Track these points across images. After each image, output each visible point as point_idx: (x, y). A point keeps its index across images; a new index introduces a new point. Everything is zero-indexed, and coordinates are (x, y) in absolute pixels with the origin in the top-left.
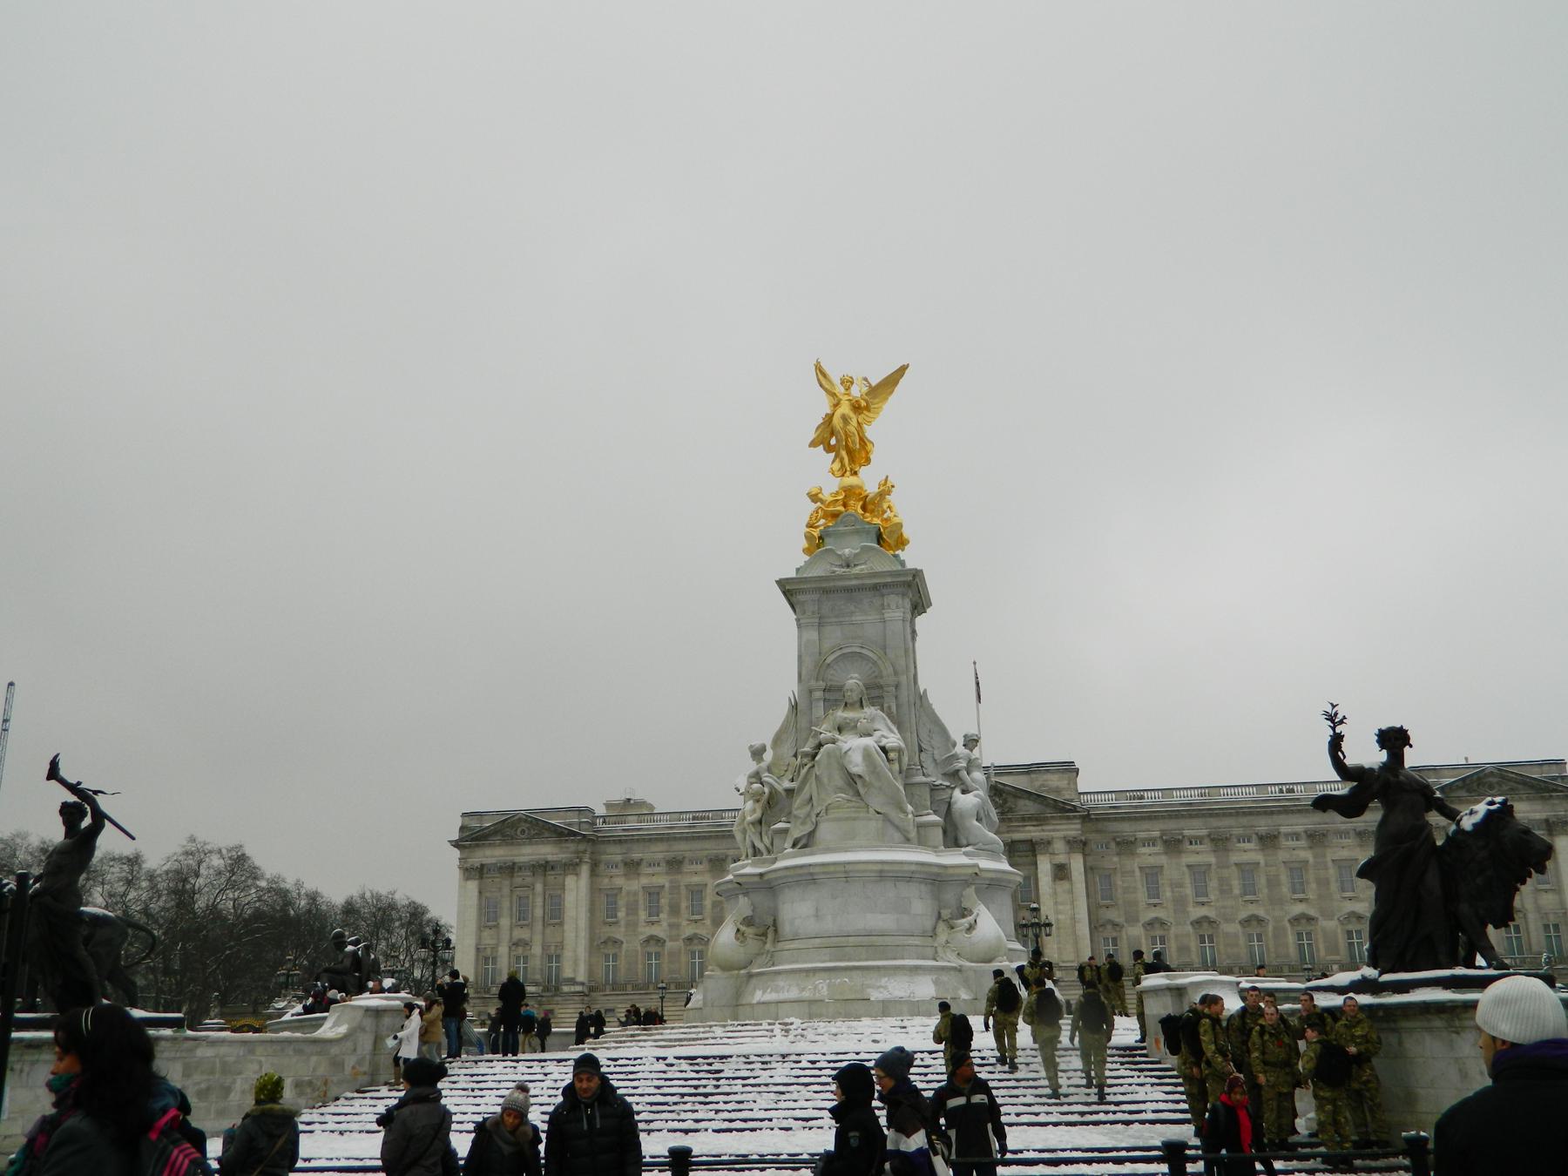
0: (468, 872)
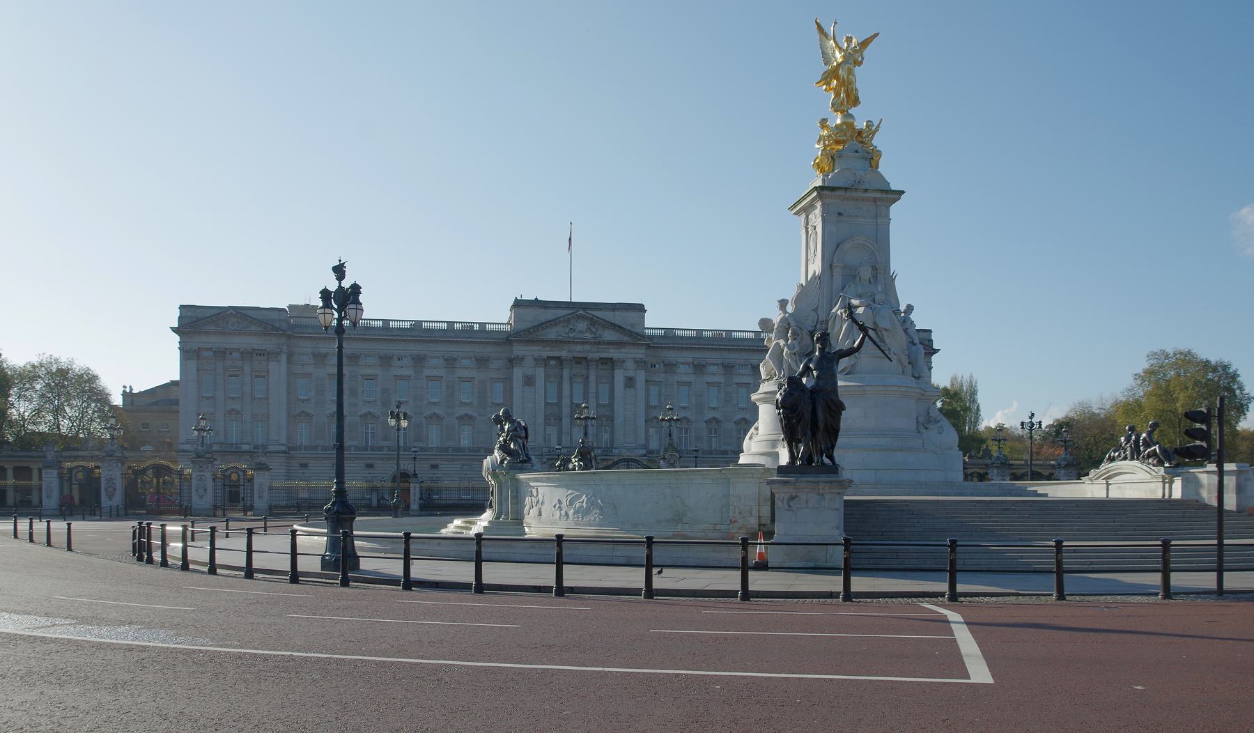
0: (187, 354)
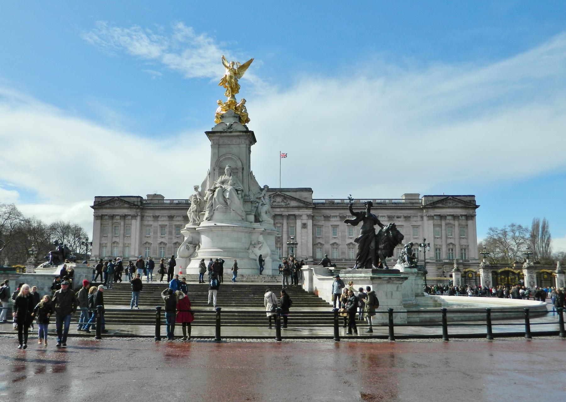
0: (97, 217)
